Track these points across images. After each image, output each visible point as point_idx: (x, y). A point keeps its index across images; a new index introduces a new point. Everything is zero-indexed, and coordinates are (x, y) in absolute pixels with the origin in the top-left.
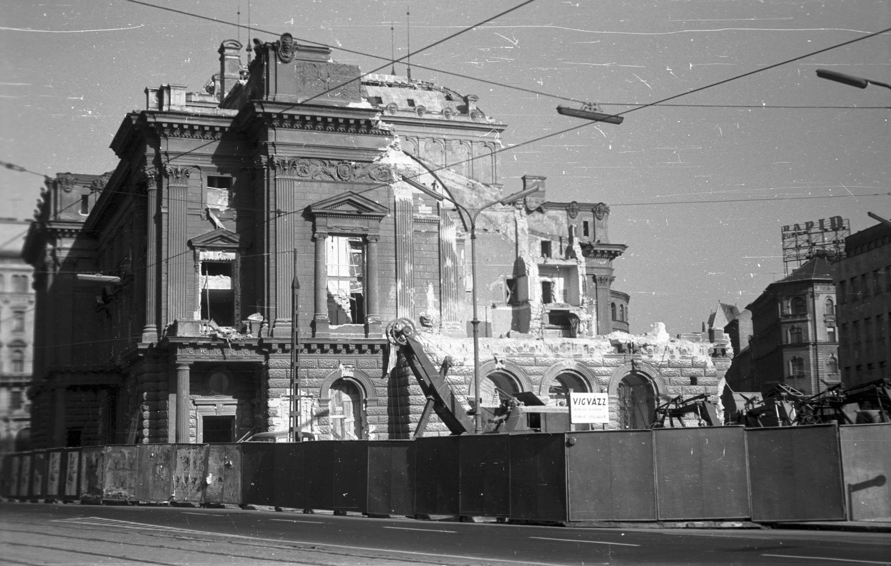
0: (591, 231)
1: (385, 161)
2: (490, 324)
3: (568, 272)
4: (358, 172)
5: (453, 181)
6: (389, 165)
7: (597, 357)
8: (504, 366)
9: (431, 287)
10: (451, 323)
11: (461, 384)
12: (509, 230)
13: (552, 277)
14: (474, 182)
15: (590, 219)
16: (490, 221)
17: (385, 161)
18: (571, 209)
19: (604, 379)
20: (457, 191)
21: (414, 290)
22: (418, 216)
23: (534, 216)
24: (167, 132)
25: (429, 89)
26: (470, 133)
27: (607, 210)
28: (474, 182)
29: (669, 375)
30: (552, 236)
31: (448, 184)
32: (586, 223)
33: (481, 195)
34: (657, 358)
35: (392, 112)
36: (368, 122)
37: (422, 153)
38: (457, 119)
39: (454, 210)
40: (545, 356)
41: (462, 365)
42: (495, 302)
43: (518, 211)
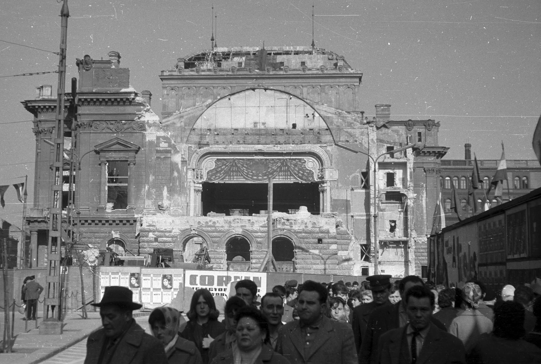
0: (423, 138)
1: (142, 119)
2: (349, 201)
3: (403, 166)
4: (126, 126)
5: (326, 111)
6: (144, 121)
7: (256, 227)
8: (196, 233)
9: (165, 188)
10: (175, 208)
11: (170, 242)
12: (363, 141)
13: (394, 169)
14: (340, 111)
15: (422, 130)
16: (351, 135)
17: (142, 119)
18: (409, 124)
19: (259, 240)
20: (328, 117)
21: (155, 190)
22: (158, 149)
23: (382, 131)
24: (40, 110)
25: (324, 53)
26: (337, 80)
27: (438, 125)
28: (340, 111)
29: (303, 238)
30: (395, 143)
31: (322, 113)
32: (420, 134)
33: (345, 119)
34: (296, 228)
35: (286, 71)
36: (128, 99)
37: (305, 95)
38: (329, 73)
39: (327, 130)
40: (222, 227)
41: (170, 232)
42: (353, 187)
43: (371, 128)
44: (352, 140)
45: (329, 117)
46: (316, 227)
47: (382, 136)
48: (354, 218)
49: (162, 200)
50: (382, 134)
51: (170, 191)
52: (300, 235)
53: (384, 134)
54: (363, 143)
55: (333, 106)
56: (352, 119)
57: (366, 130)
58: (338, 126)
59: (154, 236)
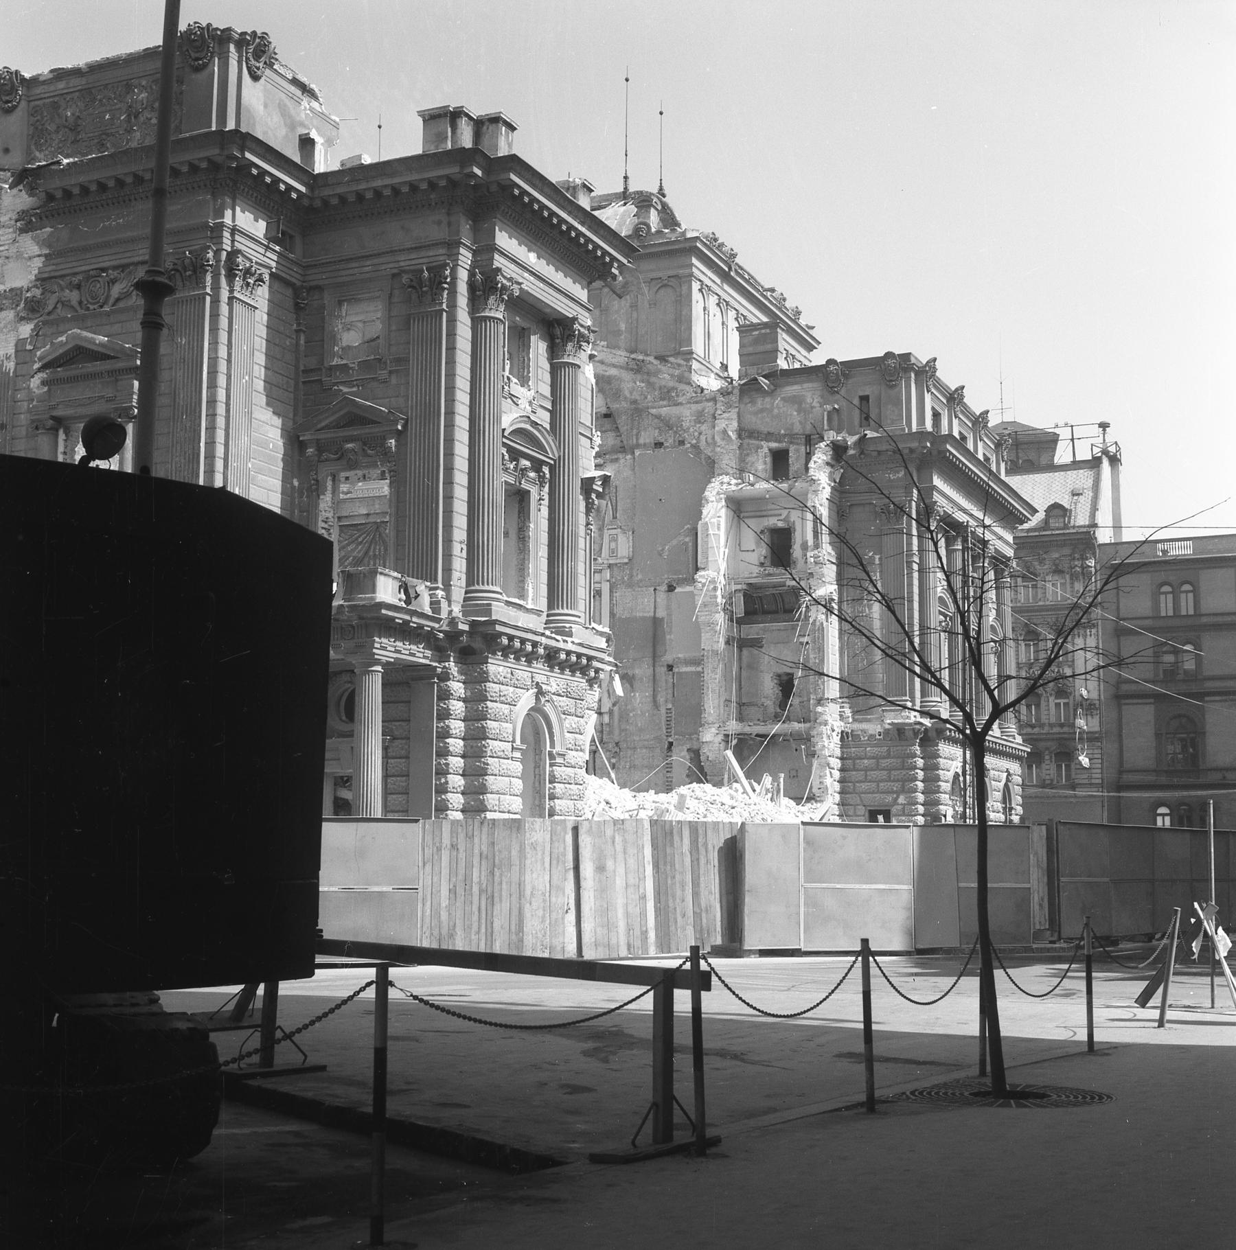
12: (703, 438)
16: (667, 424)
28: (641, 357)
33: (653, 379)
44: (671, 441)
45: (609, 377)
47: (754, 419)
48: (675, 670)
50: (756, 413)
53: (762, 411)
54: (703, 444)
55: (622, 344)
56: (672, 376)
57: (710, 404)
58: (635, 402)
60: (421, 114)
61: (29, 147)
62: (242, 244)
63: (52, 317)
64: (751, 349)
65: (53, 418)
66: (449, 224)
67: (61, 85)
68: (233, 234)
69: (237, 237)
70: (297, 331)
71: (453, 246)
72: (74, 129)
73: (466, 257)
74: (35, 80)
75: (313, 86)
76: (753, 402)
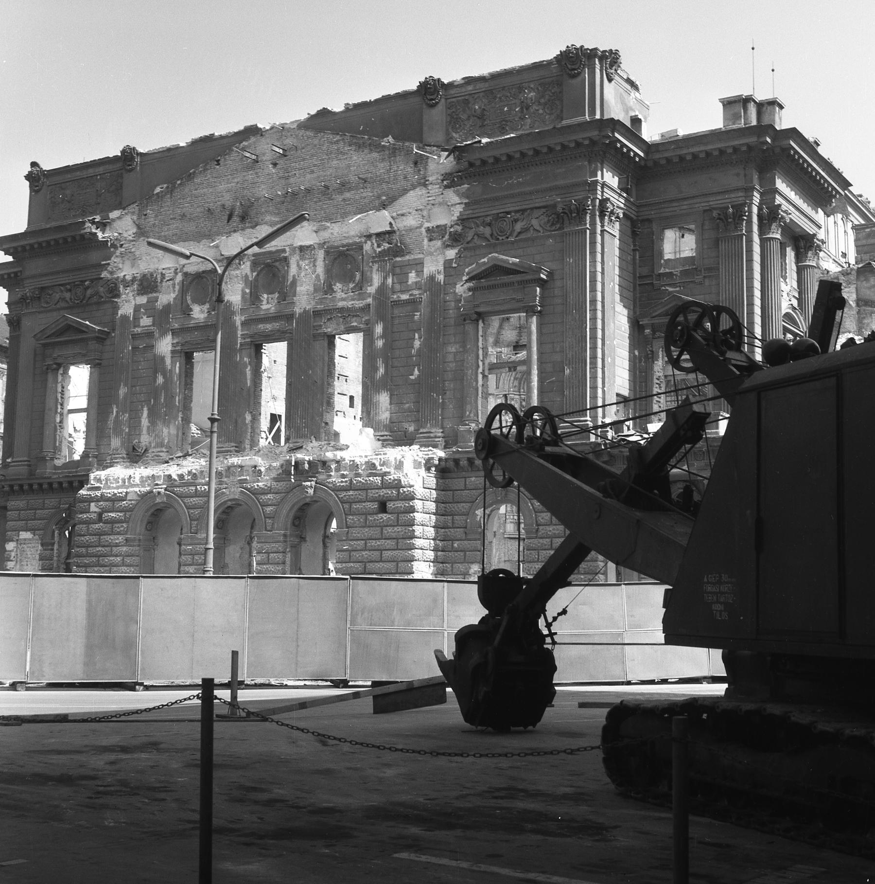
4: (89, 292)
9: (145, 409)
46: (375, 475)
47: (868, 292)
49: (140, 435)
50: (870, 288)
51: (152, 415)
52: (342, 494)
59: (97, 510)
60: (722, 101)
61: (447, 130)
62: (608, 194)
63: (471, 245)
64: (864, 242)
65: (477, 313)
66: (745, 175)
67: (470, 88)
68: (602, 188)
69: (605, 190)
70: (634, 250)
71: (748, 191)
72: (481, 117)
73: (757, 198)
74: (451, 85)
75: (637, 83)
76: (867, 280)
